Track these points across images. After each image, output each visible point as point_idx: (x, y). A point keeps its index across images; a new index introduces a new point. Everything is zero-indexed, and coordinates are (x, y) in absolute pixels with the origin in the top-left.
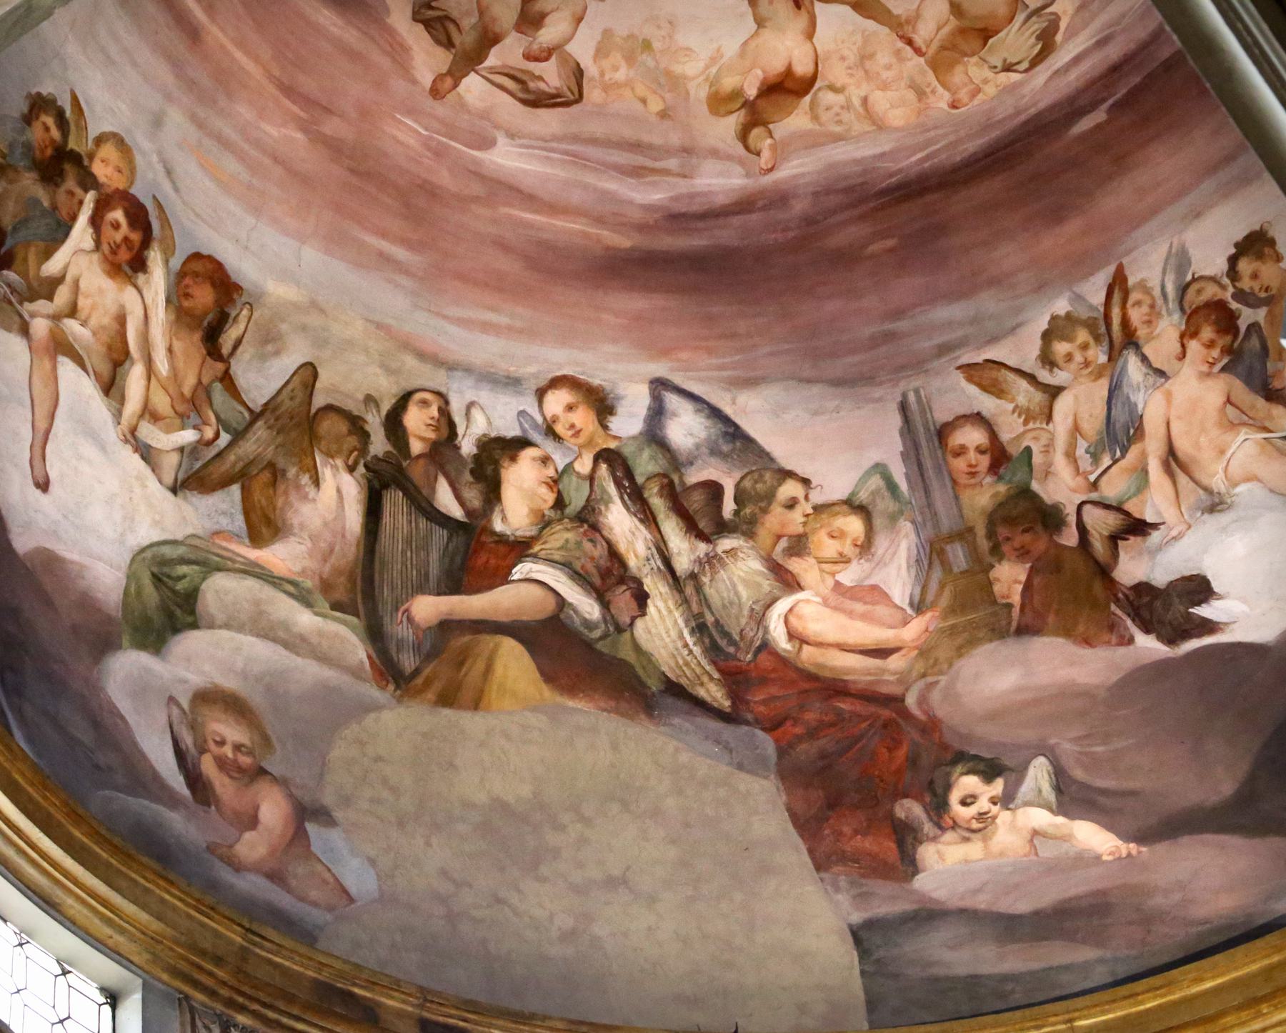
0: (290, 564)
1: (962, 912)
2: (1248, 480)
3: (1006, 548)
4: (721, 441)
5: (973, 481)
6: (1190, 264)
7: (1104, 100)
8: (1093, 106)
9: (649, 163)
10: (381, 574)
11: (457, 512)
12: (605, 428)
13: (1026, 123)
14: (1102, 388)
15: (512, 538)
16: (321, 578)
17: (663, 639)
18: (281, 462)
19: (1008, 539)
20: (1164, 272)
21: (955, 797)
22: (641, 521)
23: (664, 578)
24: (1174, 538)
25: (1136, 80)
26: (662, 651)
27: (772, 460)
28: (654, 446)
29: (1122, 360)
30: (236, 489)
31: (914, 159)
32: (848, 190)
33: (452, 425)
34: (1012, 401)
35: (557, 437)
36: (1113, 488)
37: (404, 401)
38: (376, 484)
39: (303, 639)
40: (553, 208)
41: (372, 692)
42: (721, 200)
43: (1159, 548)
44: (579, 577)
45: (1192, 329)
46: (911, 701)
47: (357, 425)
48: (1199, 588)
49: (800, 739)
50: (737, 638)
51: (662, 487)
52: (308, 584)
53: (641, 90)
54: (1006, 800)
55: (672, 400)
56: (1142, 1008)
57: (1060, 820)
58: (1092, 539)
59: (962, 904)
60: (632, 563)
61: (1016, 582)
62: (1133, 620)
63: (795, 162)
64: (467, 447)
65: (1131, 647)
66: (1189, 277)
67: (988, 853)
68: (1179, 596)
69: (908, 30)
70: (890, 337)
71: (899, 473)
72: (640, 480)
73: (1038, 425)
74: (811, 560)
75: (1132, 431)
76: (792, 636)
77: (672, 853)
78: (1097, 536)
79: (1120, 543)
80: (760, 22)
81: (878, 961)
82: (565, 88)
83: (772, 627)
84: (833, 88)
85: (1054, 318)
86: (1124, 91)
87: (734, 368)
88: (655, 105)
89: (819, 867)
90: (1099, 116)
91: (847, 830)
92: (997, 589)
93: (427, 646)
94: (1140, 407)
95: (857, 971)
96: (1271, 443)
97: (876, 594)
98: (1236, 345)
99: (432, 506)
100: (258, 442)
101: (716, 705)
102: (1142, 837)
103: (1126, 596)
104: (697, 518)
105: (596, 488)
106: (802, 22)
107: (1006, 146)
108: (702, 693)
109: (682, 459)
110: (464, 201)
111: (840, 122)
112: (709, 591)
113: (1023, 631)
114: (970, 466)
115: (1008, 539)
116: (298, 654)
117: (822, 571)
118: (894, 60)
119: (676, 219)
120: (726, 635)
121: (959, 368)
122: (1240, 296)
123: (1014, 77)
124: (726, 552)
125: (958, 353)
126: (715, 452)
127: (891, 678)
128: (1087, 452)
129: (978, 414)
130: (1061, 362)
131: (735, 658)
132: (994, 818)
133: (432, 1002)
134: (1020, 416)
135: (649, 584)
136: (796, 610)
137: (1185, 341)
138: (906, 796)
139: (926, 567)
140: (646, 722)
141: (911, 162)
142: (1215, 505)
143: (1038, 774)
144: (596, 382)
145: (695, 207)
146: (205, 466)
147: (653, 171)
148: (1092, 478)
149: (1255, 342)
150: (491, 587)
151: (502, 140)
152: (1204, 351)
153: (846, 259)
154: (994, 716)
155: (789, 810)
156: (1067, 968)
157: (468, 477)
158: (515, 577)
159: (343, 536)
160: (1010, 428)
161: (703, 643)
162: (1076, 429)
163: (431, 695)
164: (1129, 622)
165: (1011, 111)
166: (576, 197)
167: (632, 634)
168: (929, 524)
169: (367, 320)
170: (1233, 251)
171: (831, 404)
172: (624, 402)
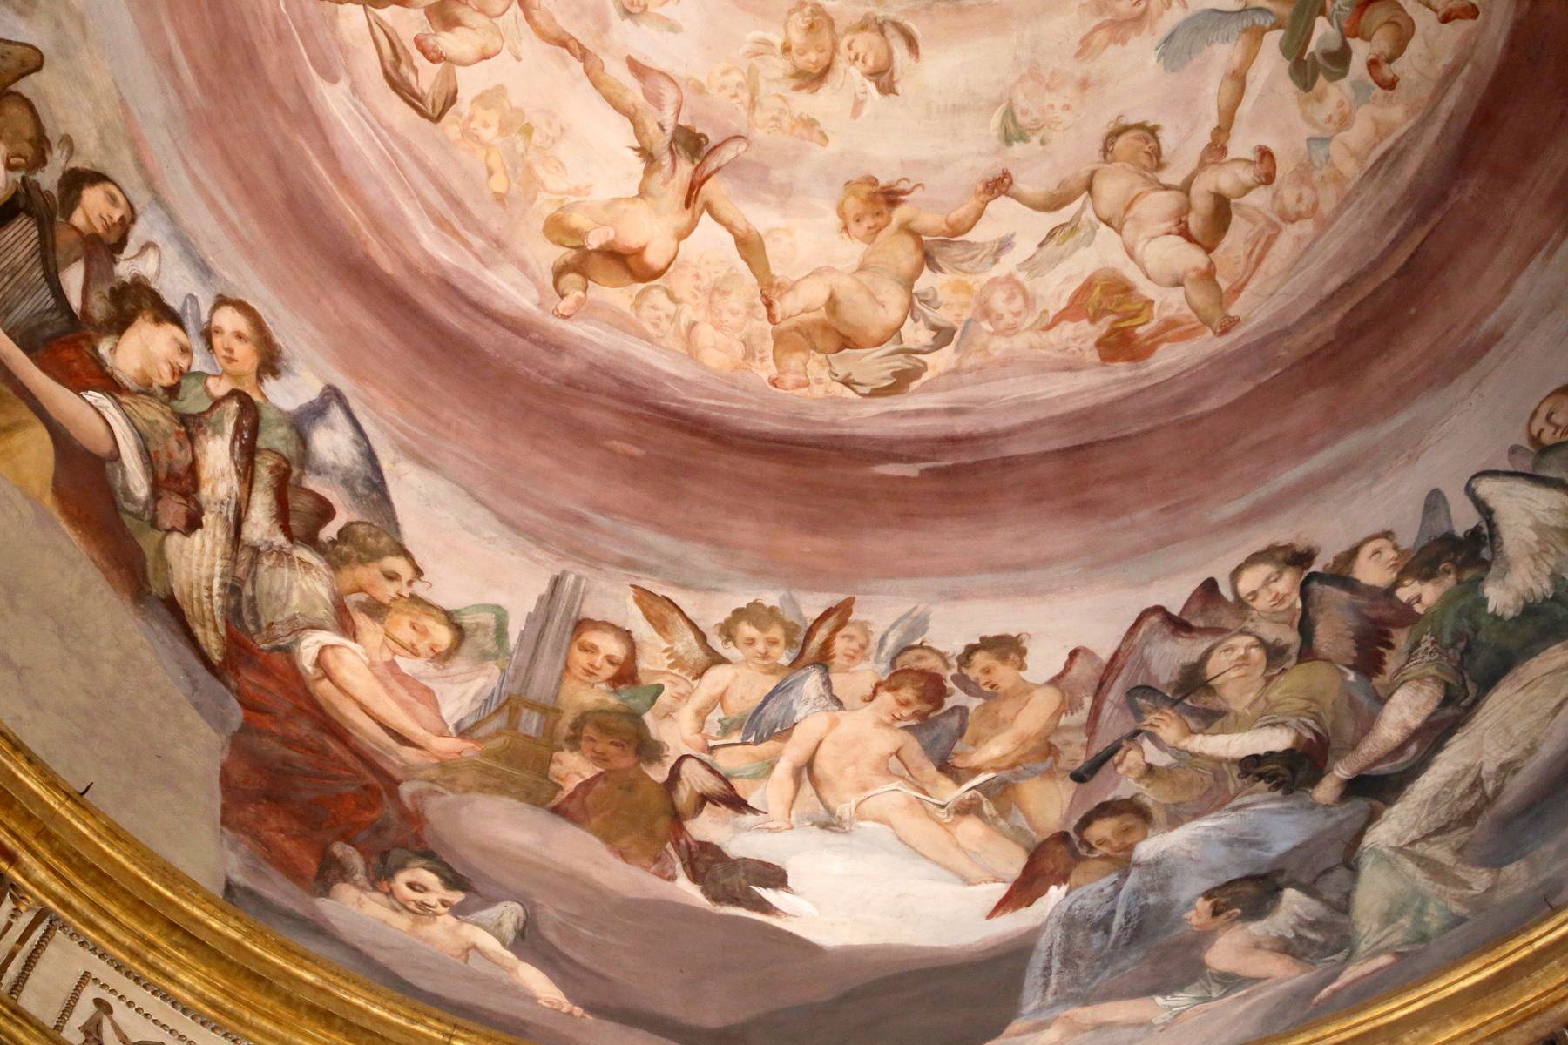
4: (360, 481)
5: (586, 678)
6: (924, 633)
7: (924, 460)
8: (911, 459)
9: (458, 226)
11: (75, 301)
12: (260, 380)
13: (837, 437)
14: (769, 683)
17: (190, 566)
19: (592, 739)
20: (893, 626)
22: (238, 472)
23: (228, 528)
24: (770, 830)
25: (966, 459)
26: (183, 576)
29: (803, 672)
32: (623, 383)
33: (122, 243)
34: (670, 642)
35: (209, 344)
37: (97, 178)
38: (22, 202)
42: (500, 305)
44: (149, 459)
45: (893, 684)
48: (776, 877)
49: (273, 735)
51: (277, 467)
53: (495, 161)
54: (458, 911)
55: (336, 414)
57: (509, 954)
58: (680, 787)
60: (205, 492)
62: (684, 866)
63: (591, 328)
64: (125, 269)
65: (669, 883)
66: (917, 642)
70: (580, 520)
71: (515, 628)
72: (260, 443)
73: (683, 674)
74: (379, 628)
75: (777, 730)
76: (319, 663)
77: (82, 699)
78: (688, 788)
80: (643, 193)
82: (430, 100)
83: (305, 643)
85: (756, 604)
86: (949, 463)
88: (498, 184)
89: (224, 822)
90: (911, 470)
92: (554, 768)
94: (797, 718)
96: (921, 803)
97: (429, 697)
98: (932, 715)
99: (57, 273)
101: (205, 649)
102: (590, 1008)
103: (689, 846)
104: (292, 515)
105: (215, 412)
106: (684, 219)
107: (803, 445)
108: (199, 631)
110: (273, 98)
111: (656, 326)
113: (556, 811)
114: (592, 666)
115: (592, 739)
118: (744, 310)
119: (448, 288)
122: (962, 680)
123: (848, 393)
124: (301, 561)
125: (644, 575)
126: (348, 482)
127: (398, 762)
128: (719, 721)
129: (629, 632)
130: (740, 638)
131: (251, 635)
132: (436, 914)
134: (669, 657)
135: (208, 518)
137: (879, 689)
139: (492, 710)
140: (129, 605)
141: (702, 403)
142: (830, 823)
144: (278, 340)
145: (474, 293)
147: (456, 233)
148: (712, 743)
151: (343, 86)
152: (895, 705)
153: (586, 436)
155: (223, 768)
157: (106, 292)
158: (88, 398)
160: (653, 659)
161: (228, 602)
162: (721, 698)
164: (679, 865)
165: (827, 419)
166: (371, 192)
167: (164, 538)
170: (977, 641)
172: (292, 378)
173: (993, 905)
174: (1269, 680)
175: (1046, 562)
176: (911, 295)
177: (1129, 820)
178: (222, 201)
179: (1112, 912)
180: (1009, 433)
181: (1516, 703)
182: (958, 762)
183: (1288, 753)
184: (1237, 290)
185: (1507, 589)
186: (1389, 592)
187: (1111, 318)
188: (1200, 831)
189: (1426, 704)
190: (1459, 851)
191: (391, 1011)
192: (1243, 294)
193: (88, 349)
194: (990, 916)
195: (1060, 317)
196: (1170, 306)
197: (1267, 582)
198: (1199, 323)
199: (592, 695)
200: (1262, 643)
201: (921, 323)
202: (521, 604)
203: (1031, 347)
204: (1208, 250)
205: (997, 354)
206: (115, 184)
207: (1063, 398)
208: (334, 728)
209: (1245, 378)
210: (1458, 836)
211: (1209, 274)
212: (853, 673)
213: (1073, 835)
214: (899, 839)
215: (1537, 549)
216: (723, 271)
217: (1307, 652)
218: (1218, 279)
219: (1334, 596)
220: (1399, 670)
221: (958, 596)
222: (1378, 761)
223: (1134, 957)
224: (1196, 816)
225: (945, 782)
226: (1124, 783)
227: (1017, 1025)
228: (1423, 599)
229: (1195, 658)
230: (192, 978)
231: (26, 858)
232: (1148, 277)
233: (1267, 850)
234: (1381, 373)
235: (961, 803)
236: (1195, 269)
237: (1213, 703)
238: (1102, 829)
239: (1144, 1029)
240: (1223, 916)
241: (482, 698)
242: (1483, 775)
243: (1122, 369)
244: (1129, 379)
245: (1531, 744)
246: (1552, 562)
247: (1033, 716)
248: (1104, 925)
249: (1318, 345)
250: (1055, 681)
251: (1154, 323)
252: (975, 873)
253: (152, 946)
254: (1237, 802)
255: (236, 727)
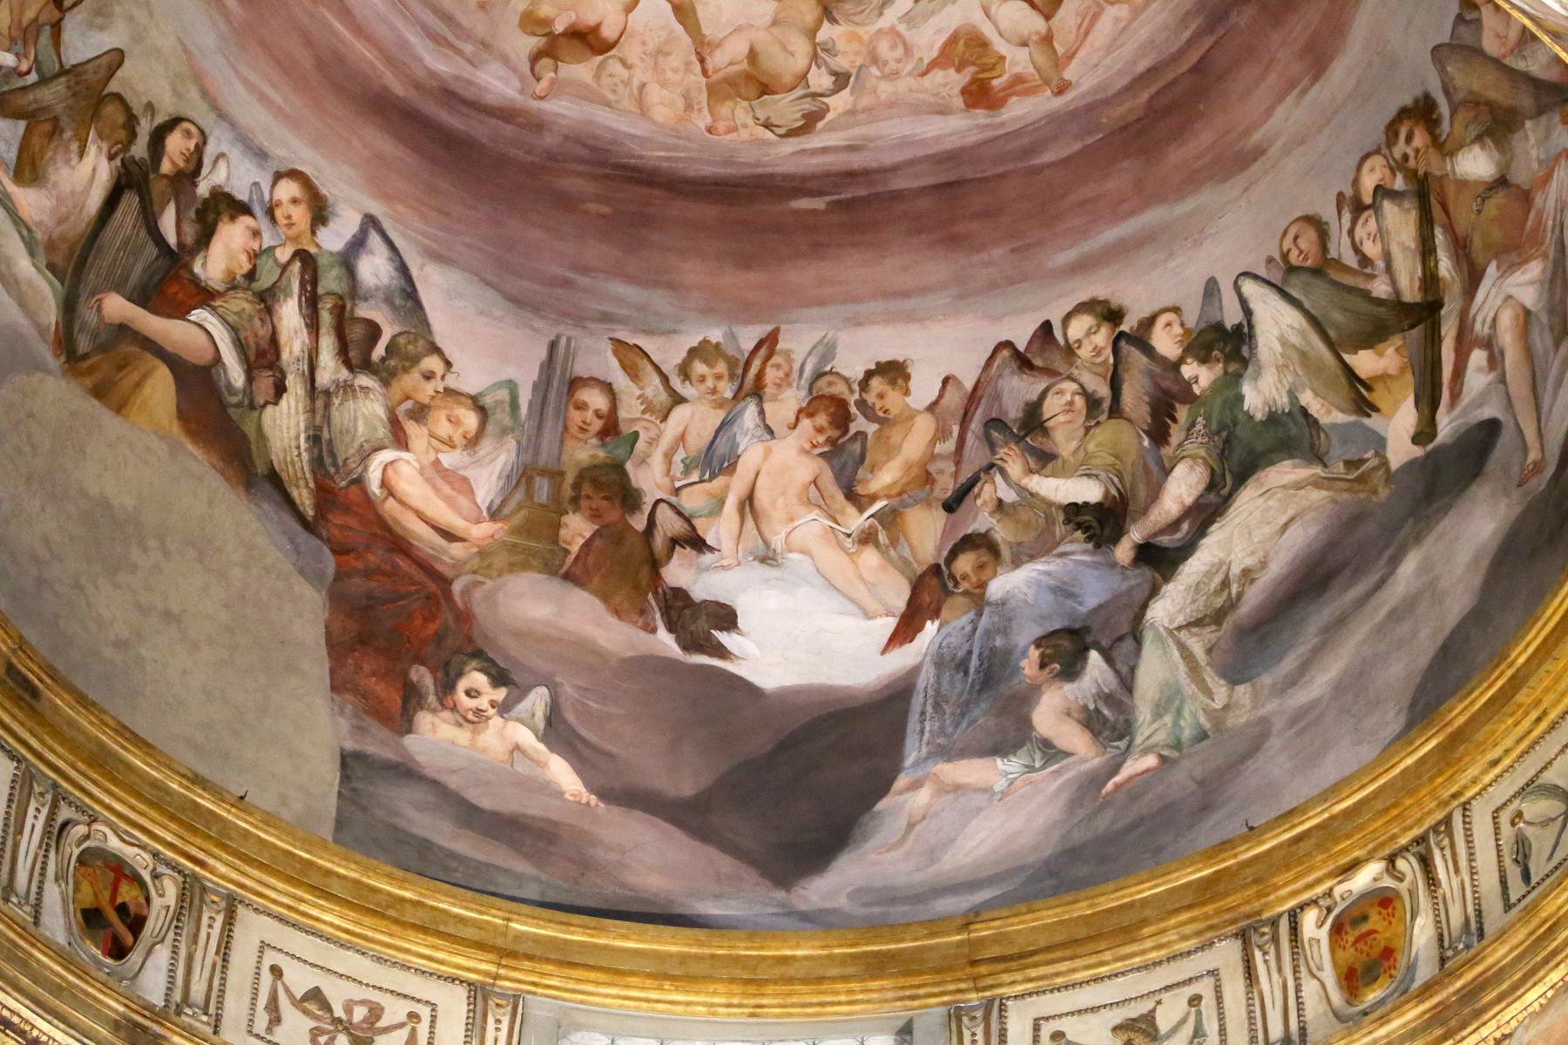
0: (33, 213)
1: (434, 783)
2: (802, 552)
3: (584, 503)
4: (397, 294)
5: (581, 436)
7: (830, 194)
8: (819, 193)
9: (451, 38)
10: (95, 259)
11: (172, 239)
12: (314, 233)
13: (760, 176)
14: (717, 417)
15: (203, 284)
16: (50, 238)
18: (64, 121)
20: (810, 353)
21: (462, 685)
22: (306, 324)
26: (278, 444)
27: (430, 332)
28: (344, 270)
30: (22, 124)
31: (657, 154)
32: (593, 149)
34: (642, 388)
35: (273, 219)
36: (691, 501)
37: (174, 122)
39: (17, 282)
40: (359, 31)
41: (46, 353)
42: (490, 99)
43: (707, 569)
44: (240, 344)
46: (457, 587)
47: (131, 123)
48: (726, 617)
50: (341, 463)
51: (335, 306)
52: (39, 236)
54: (504, 708)
55: (374, 239)
56: (569, 937)
57: (541, 747)
58: (656, 533)
59: (437, 776)
60: (285, 356)
61: (581, 535)
64: (203, 189)
65: (651, 636)
66: (828, 368)
67: (473, 745)
68: (707, 615)
69: (706, 51)
70: (567, 283)
72: (320, 291)
73: (653, 419)
74: (425, 430)
75: (726, 464)
76: (384, 484)
77: (223, 616)
79: (678, 548)
81: (354, 790)
83: (371, 469)
84: (624, 63)
85: (705, 342)
86: (850, 196)
87: (435, 241)
89: (334, 688)
90: (819, 204)
91: (367, 668)
92: (563, 532)
93: (103, 338)
94: (741, 448)
95: (336, 789)
97: (464, 486)
98: (840, 441)
100: (56, 94)
101: (301, 509)
102: (605, 795)
104: (351, 347)
107: (735, 185)
108: (295, 493)
109: (361, 292)
112: (335, 413)
113: (568, 577)
114: (584, 422)
115: (589, 497)
116: (8, 292)
117: (429, 443)
118: (682, 67)
119: (449, 95)
120: (333, 455)
121: (611, 339)
122: (862, 404)
123: (769, 135)
124: (362, 388)
126: (388, 300)
127: (448, 560)
128: (683, 461)
129: (610, 384)
130: (694, 378)
131: (331, 478)
132: (488, 718)
133: (24, 652)
134: (642, 404)
136: (397, 464)
138: (423, 664)
140: (243, 495)
141: (653, 155)
142: (767, 558)
143: (537, 701)
144: (324, 191)
145: (467, 94)
146: (11, 92)
147: (451, 46)
148: (678, 484)
149: (856, 447)
150: (170, 316)
152: (811, 430)
153: (566, 203)
154: (518, 635)
155: (326, 627)
156: (507, 871)
157: (192, 214)
158: (192, 318)
159: (81, 211)
160: (629, 410)
162: (682, 438)
163: (88, 382)
164: (658, 615)
165: (752, 160)
166: (381, 31)
168: (531, 451)
169: (179, 39)
171: (499, 313)
172: (337, 219)
173: (885, 640)
174: (1088, 429)
175: (925, 290)
176: (815, 45)
177: (985, 557)
178: (270, 92)
179: (970, 652)
180: (895, 169)
181: (1258, 508)
182: (860, 490)
183: (1099, 505)
184: (1070, 56)
185: (1259, 391)
186: (1176, 366)
187: (972, 69)
188: (1034, 574)
189: (1198, 483)
190: (1209, 651)
191: (467, 908)
192: (1074, 61)
193: (186, 275)
194: (884, 652)
195: (933, 65)
196: (1016, 64)
197: (1089, 333)
198: (1040, 82)
199: (585, 452)
200: (1084, 392)
201: (823, 68)
202: (526, 377)
203: (911, 90)
204: (1048, 18)
205: (883, 96)
206: (189, 121)
207: (937, 139)
208: (399, 544)
209: (1076, 137)
210: (1209, 634)
211: (1048, 39)
212: (781, 400)
213: (943, 567)
214: (818, 571)
215: (1281, 363)
216: (664, 34)
217: (1116, 411)
218: (1055, 44)
219: (1136, 358)
220: (1180, 445)
221: (857, 322)
222: (1162, 532)
223: (984, 706)
224: (1032, 558)
225: (851, 510)
226: (982, 520)
227: (901, 781)
228: (1200, 381)
229: (1033, 396)
230: (330, 916)
231: (211, 861)
232: (1001, 35)
233: (1080, 604)
234: (1178, 155)
235: (863, 532)
236: (1038, 33)
237: (1047, 446)
238: (965, 563)
239: (986, 796)
240: (1047, 670)
241: (505, 474)
242: (1231, 577)
243: (981, 116)
244: (987, 126)
245: (1265, 557)
246: (1291, 380)
247: (915, 441)
248: (962, 666)
249: (1131, 118)
250: (932, 408)
251: (1005, 78)
252: (872, 605)
253: (302, 900)
254: (1061, 549)
255: (331, 579)
